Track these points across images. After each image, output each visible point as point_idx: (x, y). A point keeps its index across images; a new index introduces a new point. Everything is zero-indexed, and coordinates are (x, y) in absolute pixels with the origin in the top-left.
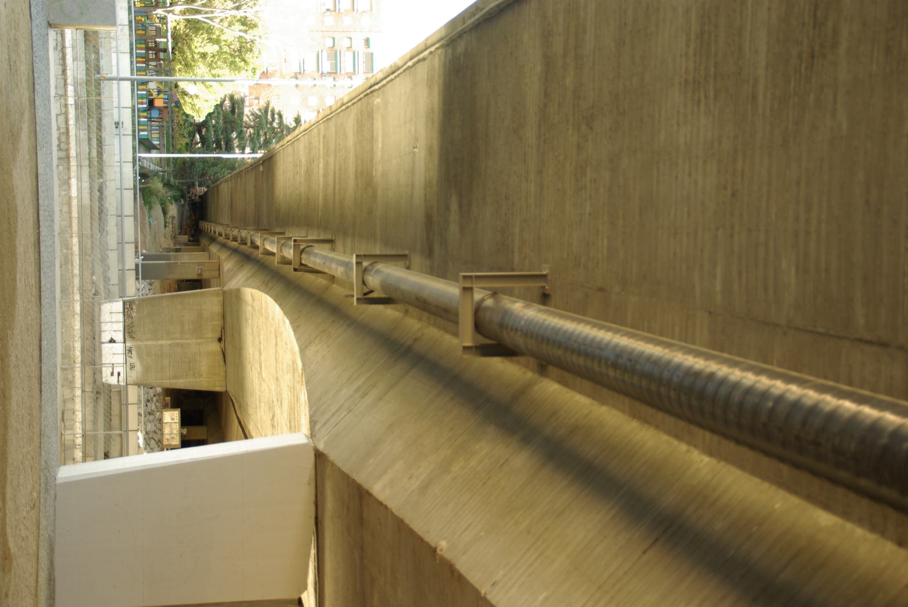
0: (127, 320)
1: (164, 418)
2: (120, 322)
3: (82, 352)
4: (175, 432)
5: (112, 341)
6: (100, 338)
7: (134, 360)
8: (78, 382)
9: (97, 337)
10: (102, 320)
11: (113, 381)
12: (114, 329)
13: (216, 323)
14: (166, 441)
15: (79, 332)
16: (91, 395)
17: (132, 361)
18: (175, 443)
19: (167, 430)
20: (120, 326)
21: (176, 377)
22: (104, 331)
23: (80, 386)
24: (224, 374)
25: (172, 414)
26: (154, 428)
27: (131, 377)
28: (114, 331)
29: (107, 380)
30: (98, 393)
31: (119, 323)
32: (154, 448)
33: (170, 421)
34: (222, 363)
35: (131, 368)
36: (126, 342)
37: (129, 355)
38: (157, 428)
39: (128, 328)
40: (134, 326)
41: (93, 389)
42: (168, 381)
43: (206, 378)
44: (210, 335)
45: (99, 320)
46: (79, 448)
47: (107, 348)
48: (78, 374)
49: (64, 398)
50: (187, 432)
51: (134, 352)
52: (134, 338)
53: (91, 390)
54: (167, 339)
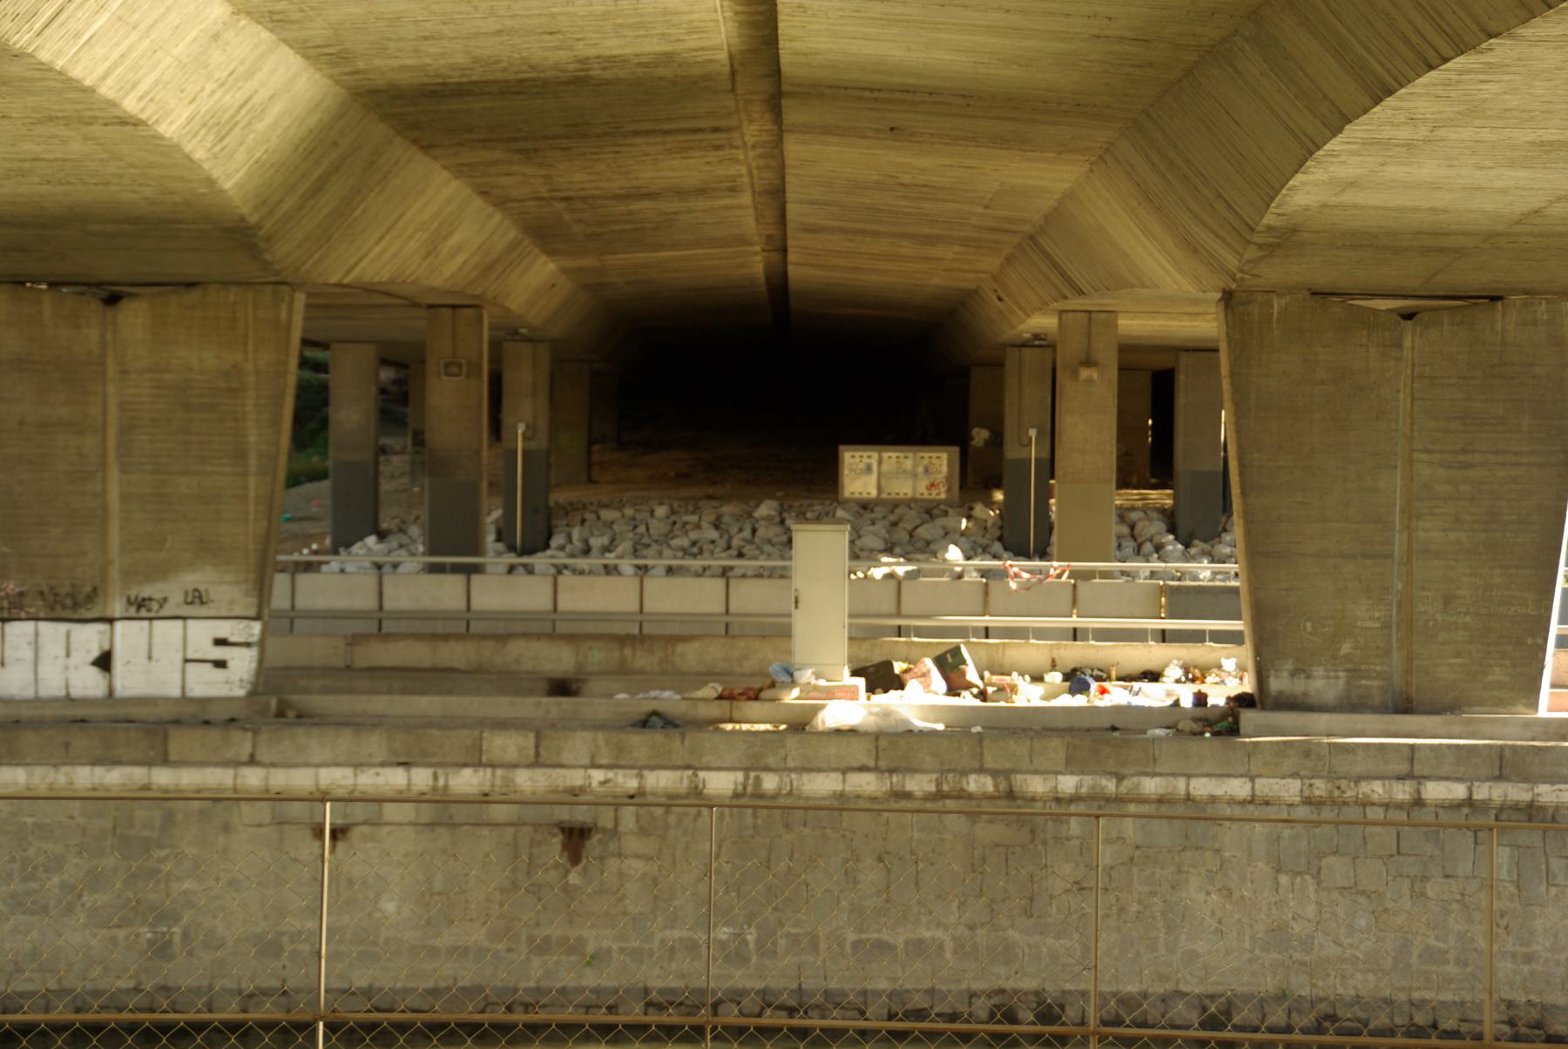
0: (32, 610)
1: (865, 495)
2: (37, 634)
3: (116, 762)
4: (909, 464)
5: (104, 662)
6: (85, 702)
7: (173, 590)
8: (217, 778)
9: (80, 712)
10: (29, 693)
11: (243, 663)
12: (62, 652)
13: (47, 309)
14: (934, 492)
15: (39, 771)
16: (265, 735)
17: (176, 598)
18: (945, 462)
19: (903, 488)
20: (52, 632)
21: (240, 455)
22: (67, 687)
23: (230, 772)
24: (234, 289)
25: (851, 470)
26: (880, 528)
27: (232, 602)
28: (68, 655)
29: (241, 680)
30: (280, 714)
31: (41, 639)
32: (943, 527)
33: (873, 478)
34: (194, 295)
35: (202, 603)
36: (108, 614)
37: (155, 606)
38: (884, 518)
39: (58, 608)
40: (52, 588)
41: (245, 730)
42: (252, 481)
43: (246, 352)
44: (93, 333)
45: (27, 701)
46: (447, 779)
47: (131, 680)
48: (188, 778)
49: (270, 825)
50: (982, 426)
51: (146, 591)
52: (95, 589)
53: (249, 735)
54: (104, 481)
